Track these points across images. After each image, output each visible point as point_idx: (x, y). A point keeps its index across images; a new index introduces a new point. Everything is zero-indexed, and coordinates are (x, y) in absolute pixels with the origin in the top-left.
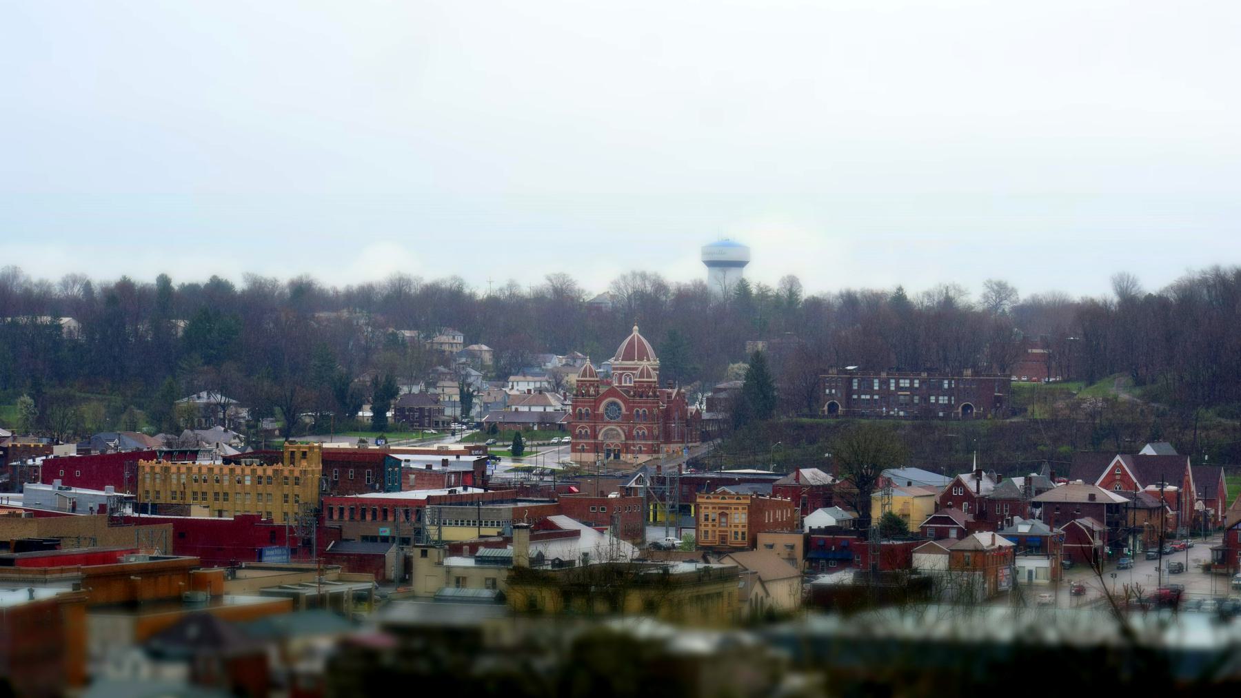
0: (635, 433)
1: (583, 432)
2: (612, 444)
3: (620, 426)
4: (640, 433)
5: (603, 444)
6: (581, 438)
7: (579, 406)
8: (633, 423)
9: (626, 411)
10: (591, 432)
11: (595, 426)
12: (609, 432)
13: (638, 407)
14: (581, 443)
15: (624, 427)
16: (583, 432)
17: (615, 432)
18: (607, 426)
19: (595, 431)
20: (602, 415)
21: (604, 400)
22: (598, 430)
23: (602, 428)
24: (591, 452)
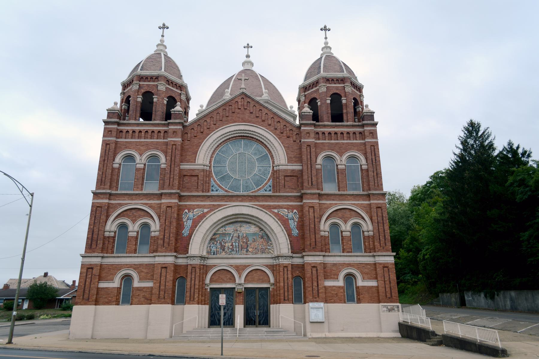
0: (325, 227)
1: (134, 228)
2: (240, 269)
3: (269, 208)
4: (346, 227)
5: (206, 269)
6: (123, 249)
7: (127, 146)
8: (320, 196)
9: (290, 160)
10: (163, 229)
11: (180, 210)
12: (230, 229)
13: (332, 147)
14: (119, 267)
15: (284, 212)
16: (134, 228)
17: (253, 229)
18: (213, 208)
19: (180, 226)
20: (208, 174)
21: (210, 130)
22: (188, 224)
23: (202, 217)
24: (161, 300)
